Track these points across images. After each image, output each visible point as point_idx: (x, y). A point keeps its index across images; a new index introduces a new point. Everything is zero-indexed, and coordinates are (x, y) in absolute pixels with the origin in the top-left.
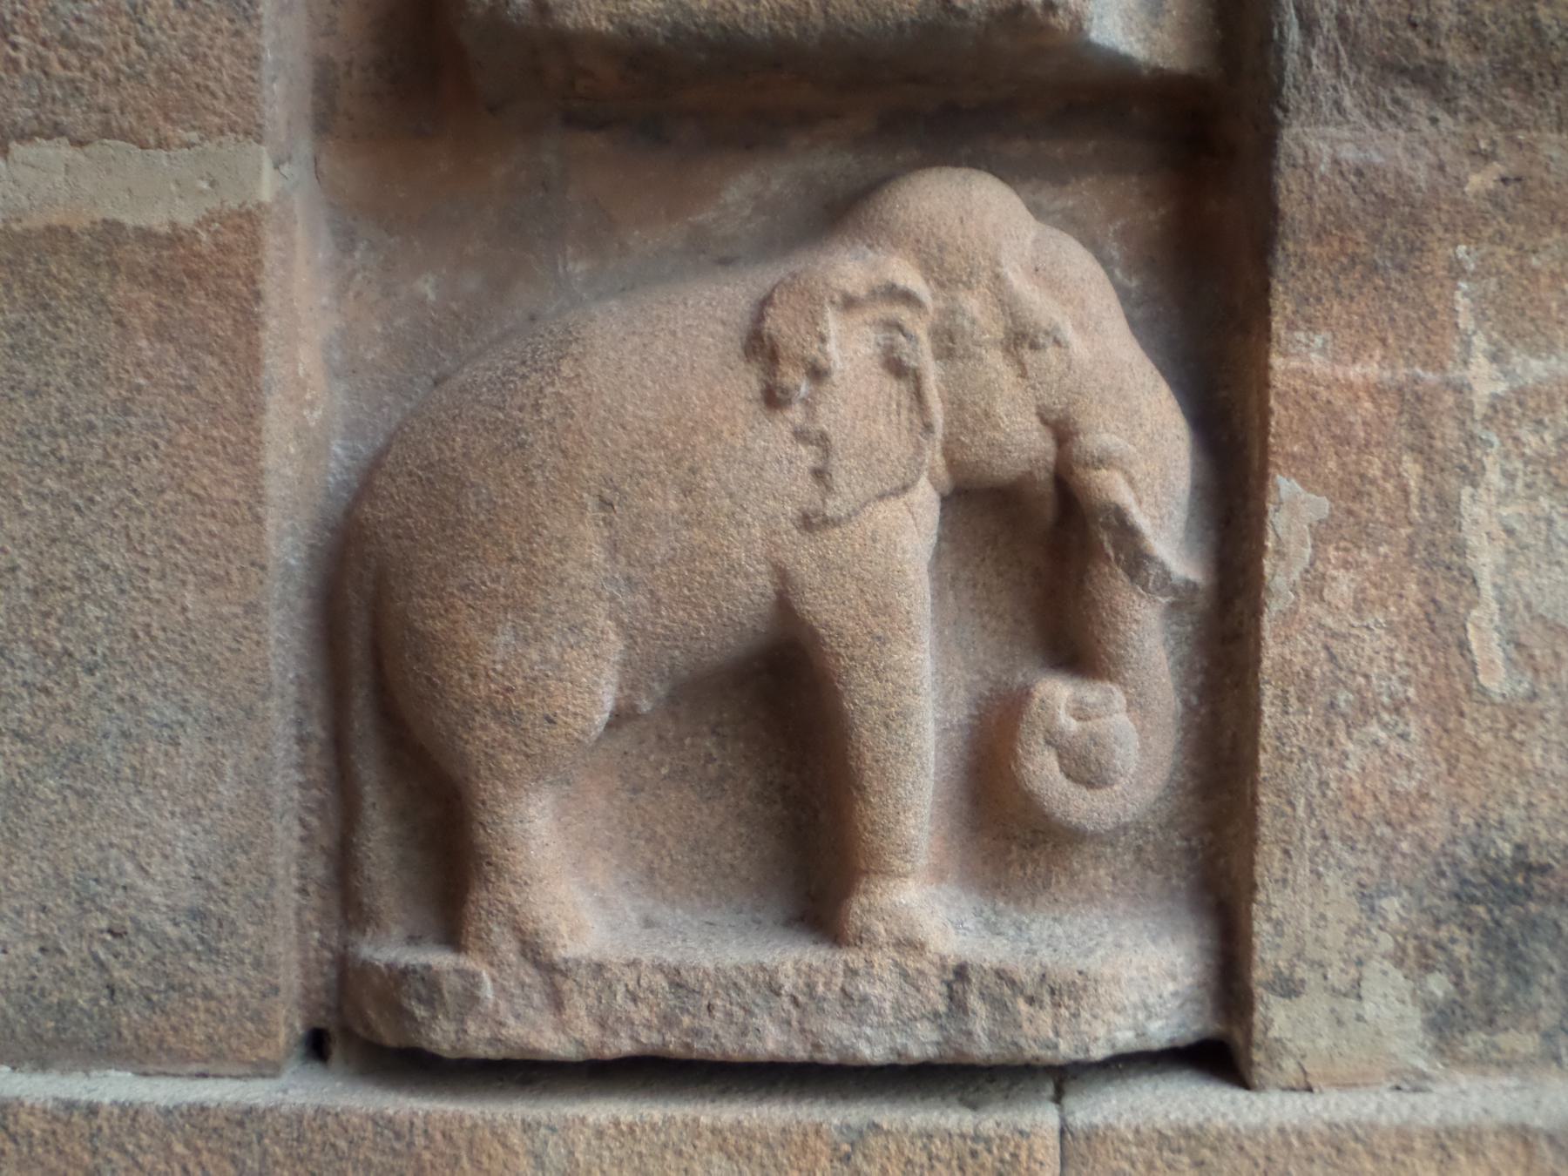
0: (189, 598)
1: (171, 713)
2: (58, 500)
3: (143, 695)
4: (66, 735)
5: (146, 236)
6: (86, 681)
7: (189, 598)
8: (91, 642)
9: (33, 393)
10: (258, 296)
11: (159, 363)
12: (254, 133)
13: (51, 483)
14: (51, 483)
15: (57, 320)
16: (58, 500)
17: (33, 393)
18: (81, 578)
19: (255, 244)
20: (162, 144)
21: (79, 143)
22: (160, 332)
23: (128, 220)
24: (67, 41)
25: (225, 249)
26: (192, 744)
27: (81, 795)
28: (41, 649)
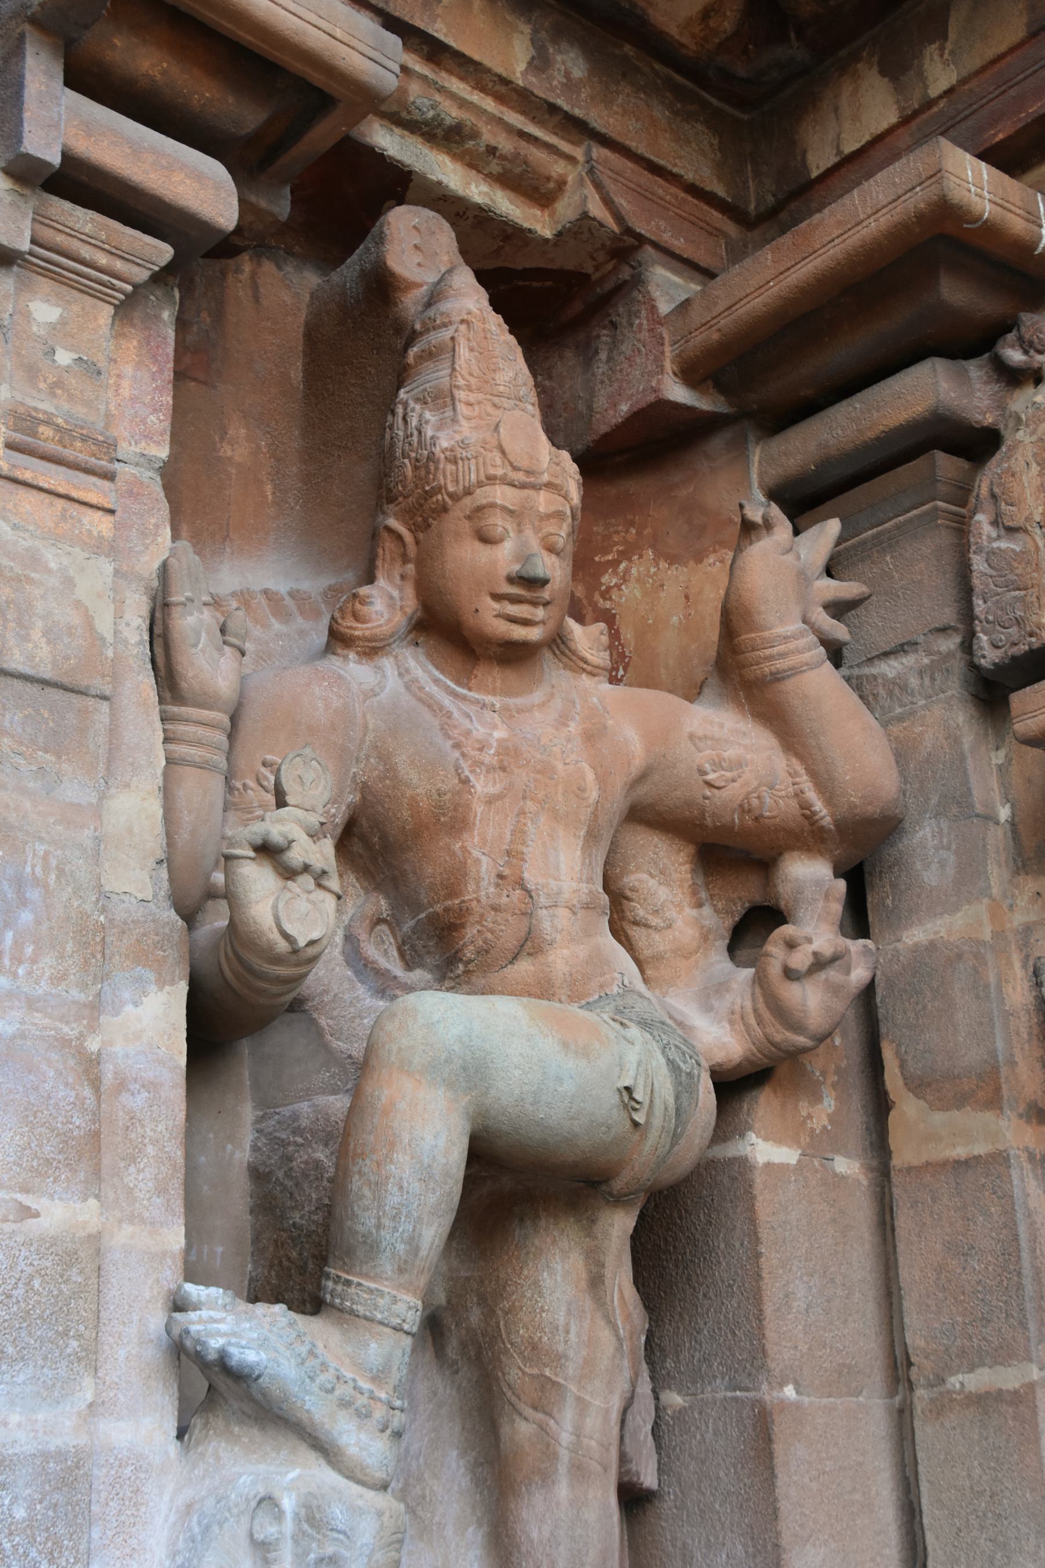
0: (1028, 1495)
1: (1027, 1530)
2: (994, 1469)
3: (1020, 1526)
4: (1002, 1539)
5: (1008, 1391)
6: (1005, 1522)
7: (1028, 1495)
8: (1005, 1510)
9: (986, 1439)
10: (1036, 1406)
11: (1014, 1427)
12: (1030, 1360)
13: (992, 1464)
14: (992, 1464)
15: (990, 1417)
16: (994, 1469)
17: (986, 1439)
18: (1001, 1491)
19: (1034, 1392)
20: (1010, 1366)
21: (990, 1367)
22: (1014, 1418)
23: (1004, 1388)
24: (984, 1339)
25: (1026, 1393)
26: (1033, 1540)
27: (1007, 1557)
28: (994, 1513)
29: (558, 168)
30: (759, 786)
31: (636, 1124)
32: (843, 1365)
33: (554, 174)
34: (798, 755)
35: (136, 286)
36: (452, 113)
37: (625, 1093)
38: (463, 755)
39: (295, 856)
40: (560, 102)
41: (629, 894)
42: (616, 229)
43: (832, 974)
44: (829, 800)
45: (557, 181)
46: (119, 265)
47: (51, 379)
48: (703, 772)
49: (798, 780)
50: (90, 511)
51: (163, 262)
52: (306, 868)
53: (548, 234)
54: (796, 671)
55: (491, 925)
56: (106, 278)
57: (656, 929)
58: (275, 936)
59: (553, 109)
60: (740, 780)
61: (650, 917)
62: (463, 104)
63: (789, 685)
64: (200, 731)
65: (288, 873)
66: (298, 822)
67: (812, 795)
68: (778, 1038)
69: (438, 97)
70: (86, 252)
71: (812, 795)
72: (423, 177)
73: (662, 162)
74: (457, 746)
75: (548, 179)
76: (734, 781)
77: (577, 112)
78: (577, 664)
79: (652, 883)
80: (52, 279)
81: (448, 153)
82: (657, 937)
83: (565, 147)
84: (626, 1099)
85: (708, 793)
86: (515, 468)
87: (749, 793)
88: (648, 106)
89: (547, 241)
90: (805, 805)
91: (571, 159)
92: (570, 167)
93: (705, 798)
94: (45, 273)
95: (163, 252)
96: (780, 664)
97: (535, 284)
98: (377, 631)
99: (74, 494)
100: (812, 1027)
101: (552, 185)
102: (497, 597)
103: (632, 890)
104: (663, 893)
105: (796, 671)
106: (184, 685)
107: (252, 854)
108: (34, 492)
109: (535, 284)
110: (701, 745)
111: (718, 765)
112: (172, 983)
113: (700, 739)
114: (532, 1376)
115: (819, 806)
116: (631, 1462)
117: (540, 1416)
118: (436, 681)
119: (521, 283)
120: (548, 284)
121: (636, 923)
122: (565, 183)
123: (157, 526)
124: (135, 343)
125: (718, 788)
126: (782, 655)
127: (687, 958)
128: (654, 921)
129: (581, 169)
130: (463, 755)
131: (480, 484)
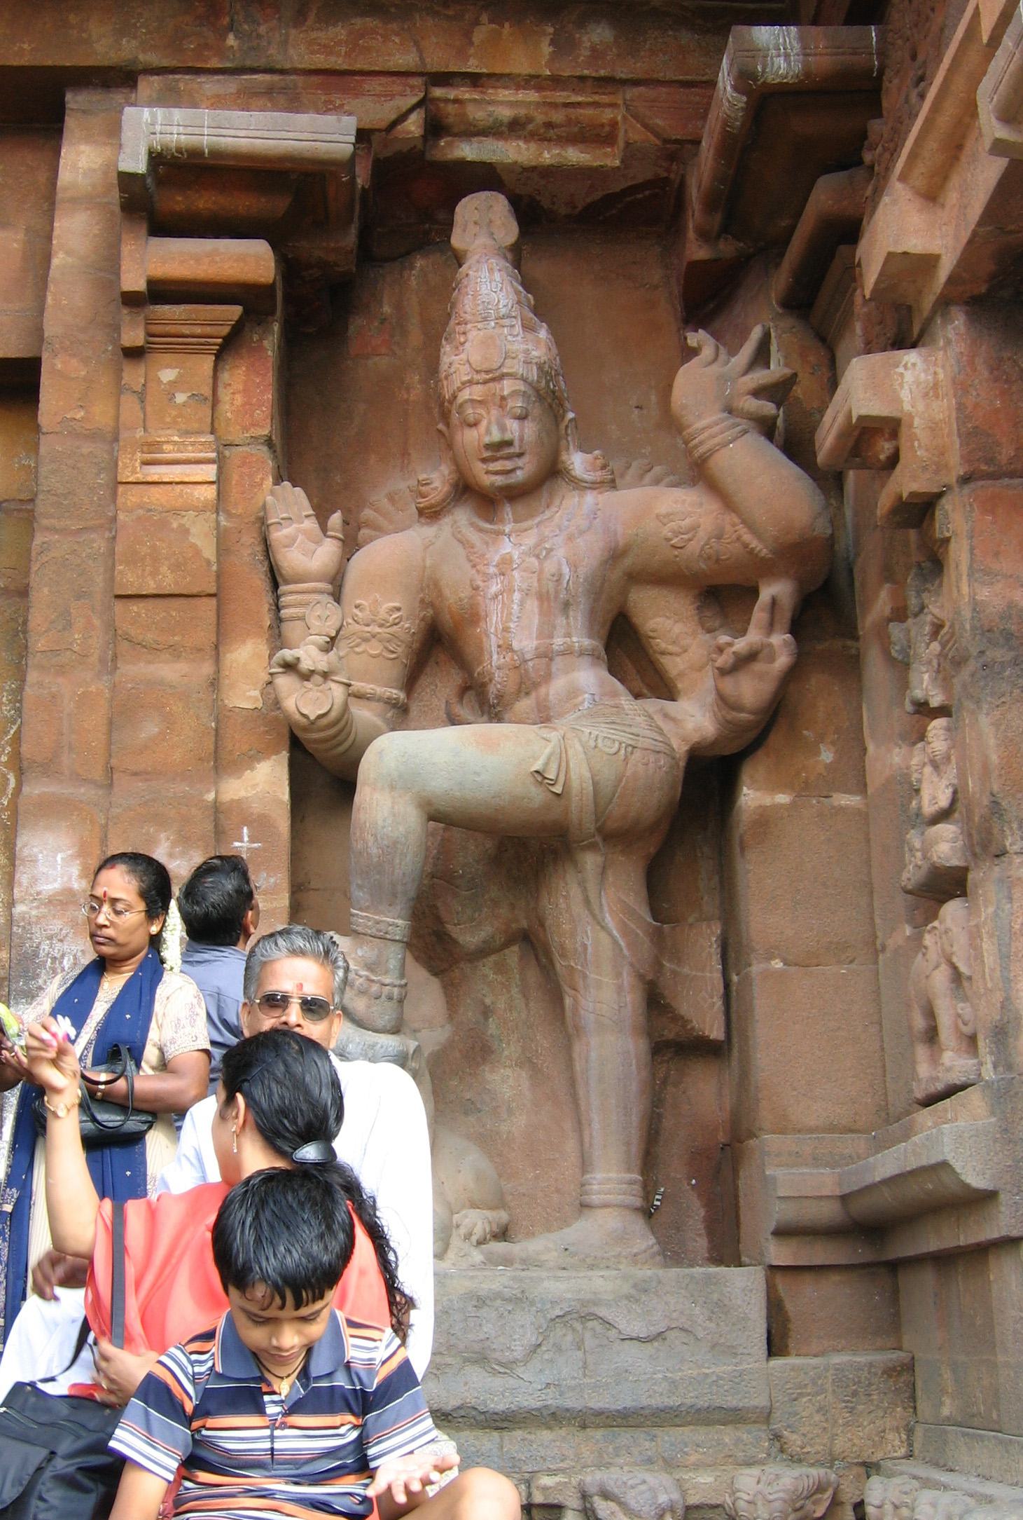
29: (607, 115)
30: (709, 539)
31: (558, 795)
32: (831, 943)
33: (605, 121)
34: (734, 511)
35: (224, 338)
36: (506, 113)
37: (536, 775)
38: (478, 571)
39: (305, 665)
40: (586, 72)
41: (651, 634)
42: (658, 142)
43: (758, 667)
44: (759, 537)
45: (609, 125)
46: (208, 330)
47: (174, 413)
48: (668, 540)
49: (737, 528)
50: (199, 487)
51: (236, 318)
52: (313, 672)
53: (617, 163)
54: (712, 452)
55: (500, 680)
56: (203, 340)
57: (677, 655)
58: (298, 717)
59: (582, 79)
60: (696, 539)
61: (670, 647)
62: (512, 104)
63: (712, 463)
64: (299, 597)
65: (306, 676)
66: (314, 643)
67: (747, 537)
68: (729, 717)
69: (491, 108)
70: (186, 330)
71: (747, 537)
72: (502, 163)
73: (689, 78)
74: (474, 566)
75: (603, 125)
76: (690, 540)
77: (602, 73)
78: (579, 485)
79: (669, 623)
80: (174, 351)
81: (519, 138)
82: (678, 659)
83: (605, 99)
84: (540, 779)
85: (676, 553)
86: (477, 372)
87: (703, 546)
88: (676, 39)
89: (618, 168)
90: (746, 546)
91: (613, 105)
92: (616, 111)
93: (676, 556)
94: (166, 351)
95: (235, 311)
96: (702, 450)
97: (640, 196)
98: (433, 501)
99: (186, 480)
100: (748, 705)
101: (607, 129)
102: (484, 460)
103: (653, 631)
104: (678, 629)
105: (712, 452)
106: (284, 572)
107: (280, 670)
108: (162, 486)
109: (640, 196)
110: (665, 521)
111: (677, 533)
112: (277, 753)
113: (664, 517)
114: (565, 966)
115: (755, 544)
116: (691, 1021)
117: (573, 992)
118: (472, 524)
119: (628, 199)
120: (647, 193)
121: (663, 653)
122: (617, 123)
123: (262, 479)
124: (244, 369)
125: (681, 548)
126: (701, 443)
127: (700, 671)
128: (671, 648)
129: (623, 109)
130: (478, 571)
131: (460, 390)
